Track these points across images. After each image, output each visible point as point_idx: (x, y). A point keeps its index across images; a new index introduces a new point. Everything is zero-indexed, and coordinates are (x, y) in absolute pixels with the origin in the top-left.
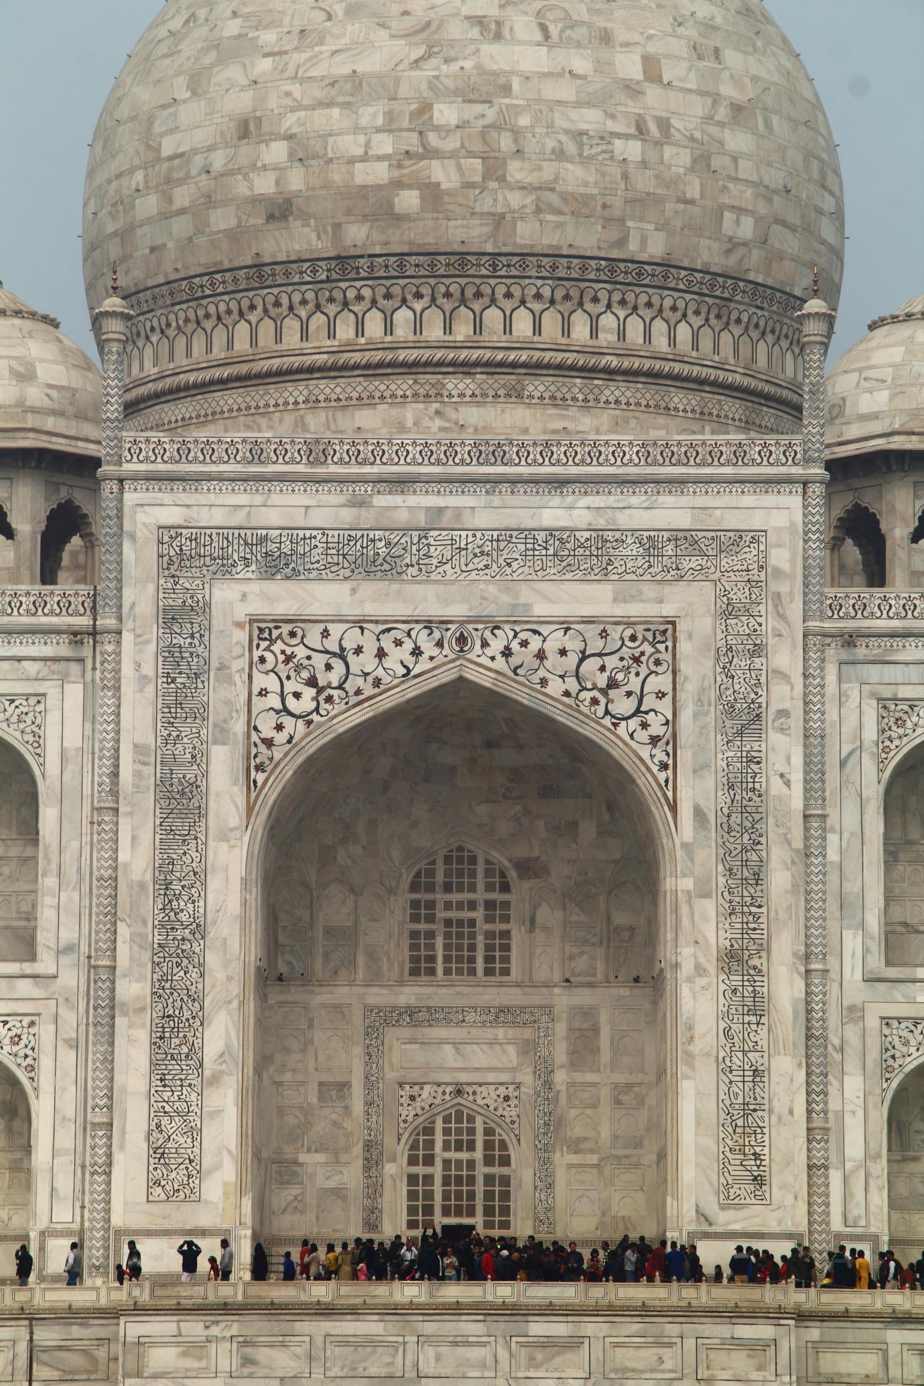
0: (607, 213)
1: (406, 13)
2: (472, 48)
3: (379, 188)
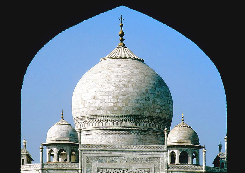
0: (141, 110)
1: (115, 84)
2: (123, 88)
3: (112, 106)
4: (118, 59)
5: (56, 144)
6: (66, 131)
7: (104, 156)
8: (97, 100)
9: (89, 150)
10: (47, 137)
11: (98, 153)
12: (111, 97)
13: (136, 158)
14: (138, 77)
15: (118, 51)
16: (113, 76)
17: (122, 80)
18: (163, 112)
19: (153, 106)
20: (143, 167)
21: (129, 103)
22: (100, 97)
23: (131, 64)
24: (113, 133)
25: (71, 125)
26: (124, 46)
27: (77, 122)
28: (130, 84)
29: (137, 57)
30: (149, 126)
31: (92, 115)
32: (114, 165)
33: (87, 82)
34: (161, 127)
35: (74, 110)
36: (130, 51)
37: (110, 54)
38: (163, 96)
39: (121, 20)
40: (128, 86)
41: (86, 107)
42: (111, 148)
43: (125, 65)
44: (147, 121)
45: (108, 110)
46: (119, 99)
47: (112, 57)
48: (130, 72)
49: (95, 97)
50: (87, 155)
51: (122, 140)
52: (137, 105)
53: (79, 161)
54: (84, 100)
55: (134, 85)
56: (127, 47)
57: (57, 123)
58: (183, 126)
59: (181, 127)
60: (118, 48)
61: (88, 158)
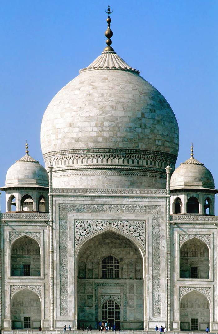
1: (99, 105)
3: (95, 137)
4: (103, 70)
5: (18, 187)
6: (31, 170)
7: (84, 203)
8: (74, 128)
9: (63, 196)
10: (6, 179)
11: (75, 199)
12: (93, 124)
13: (127, 206)
14: (130, 96)
15: (104, 59)
16: (96, 95)
17: (109, 100)
18: (165, 145)
19: (151, 136)
20: (136, 218)
21: (118, 132)
22: (79, 124)
23: (121, 77)
24: (96, 174)
25: (39, 162)
26: (112, 51)
27: (49, 159)
28: (120, 105)
29: (130, 68)
30: (146, 164)
31: (68, 149)
32: (97, 216)
33: (60, 103)
34: (162, 166)
35: (43, 142)
36: (120, 58)
37: (93, 63)
38: (165, 122)
39: (109, 13)
40: (117, 109)
41: (60, 139)
42: (93, 193)
43: (113, 79)
44: (143, 157)
45: (89, 141)
46: (105, 127)
47: (95, 68)
48: (119, 88)
49: (72, 125)
50: (61, 202)
51: (108, 183)
52: (130, 135)
53: (50, 211)
54: (58, 129)
55: (126, 107)
56: (116, 53)
57: (20, 160)
58: (192, 163)
59: (190, 164)
60: (104, 54)
61: (62, 207)
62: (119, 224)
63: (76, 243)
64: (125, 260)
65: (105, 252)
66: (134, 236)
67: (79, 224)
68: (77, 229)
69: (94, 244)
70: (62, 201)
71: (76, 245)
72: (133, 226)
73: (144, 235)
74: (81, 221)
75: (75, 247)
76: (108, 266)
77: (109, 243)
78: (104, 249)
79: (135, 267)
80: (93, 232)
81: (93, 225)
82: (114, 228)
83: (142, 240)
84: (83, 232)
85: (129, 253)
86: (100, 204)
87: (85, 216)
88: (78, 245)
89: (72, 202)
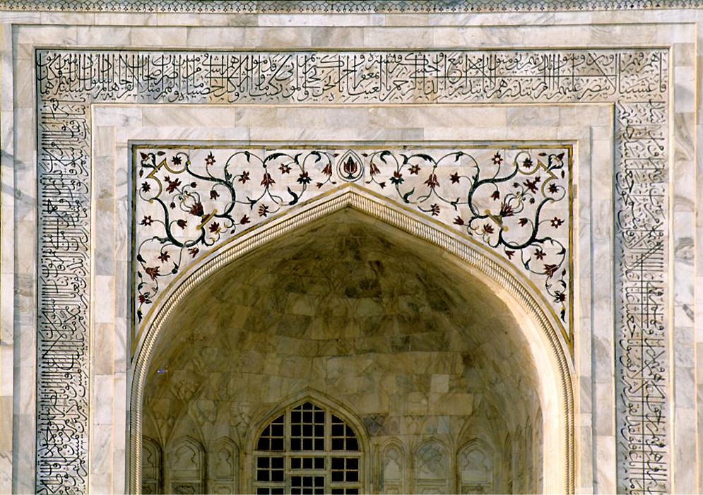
11: (139, 19)
13: (456, 56)
20: (513, 134)
32: (274, 122)
50: (48, 36)
62: (405, 172)
63: (143, 291)
64: (395, 427)
65: (276, 382)
66: (501, 240)
67: (161, 174)
68: (150, 201)
69: (224, 324)
70: (55, 29)
71: (142, 299)
72: (493, 181)
73: (560, 235)
74: (170, 155)
75: (134, 316)
76: (296, 463)
77: (307, 320)
78: (278, 361)
79: (456, 468)
80: (245, 220)
81: (245, 177)
82: (374, 195)
83: (551, 270)
84: (182, 224)
85: (424, 385)
86: (291, 51)
87: (198, 122)
88: (154, 299)
89: (120, 39)
